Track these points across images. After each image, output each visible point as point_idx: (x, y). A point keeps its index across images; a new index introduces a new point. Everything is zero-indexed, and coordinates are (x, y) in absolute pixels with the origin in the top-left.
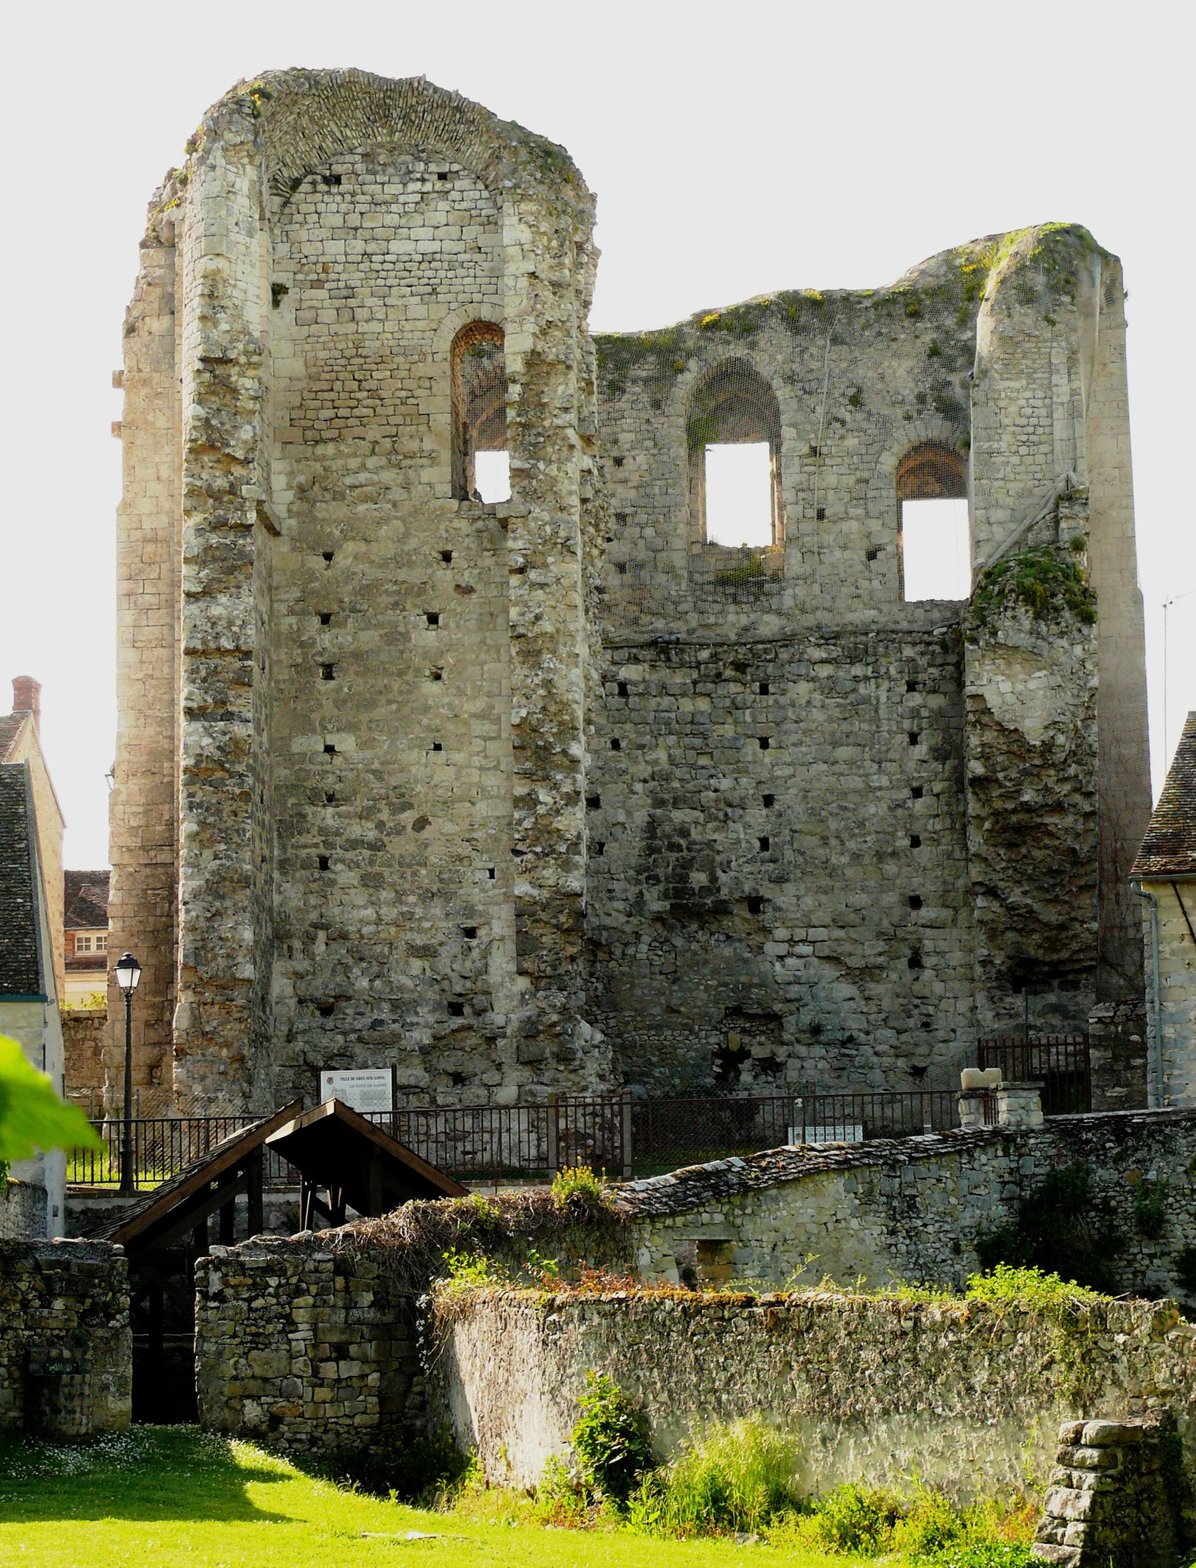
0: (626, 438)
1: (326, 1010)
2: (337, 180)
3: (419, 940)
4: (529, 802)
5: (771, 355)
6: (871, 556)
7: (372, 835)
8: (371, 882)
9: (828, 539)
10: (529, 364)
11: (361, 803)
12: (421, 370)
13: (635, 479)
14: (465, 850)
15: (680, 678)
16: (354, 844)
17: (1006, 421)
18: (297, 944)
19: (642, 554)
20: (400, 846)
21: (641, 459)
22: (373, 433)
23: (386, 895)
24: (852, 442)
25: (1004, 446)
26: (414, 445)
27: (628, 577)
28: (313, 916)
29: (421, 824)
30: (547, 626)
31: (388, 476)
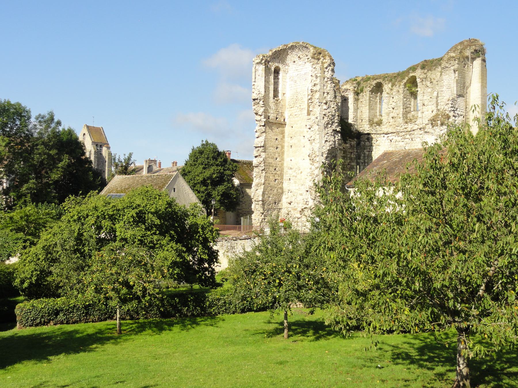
0: (394, 93)
1: (290, 204)
2: (294, 62)
3: (301, 192)
4: (311, 169)
5: (418, 74)
6: (432, 112)
7: (295, 175)
8: (295, 182)
9: (424, 110)
10: (312, 92)
11: (294, 169)
12: (304, 94)
13: (395, 101)
14: (306, 177)
15: (400, 138)
16: (293, 176)
17: (444, 84)
18: (286, 193)
19: (396, 115)
20: (299, 176)
21: (397, 97)
22: (298, 105)
23: (297, 185)
24: (429, 90)
25: (444, 90)
26: (302, 107)
27: (393, 120)
28: (288, 188)
29: (301, 172)
30: (312, 138)
31: (299, 113)
